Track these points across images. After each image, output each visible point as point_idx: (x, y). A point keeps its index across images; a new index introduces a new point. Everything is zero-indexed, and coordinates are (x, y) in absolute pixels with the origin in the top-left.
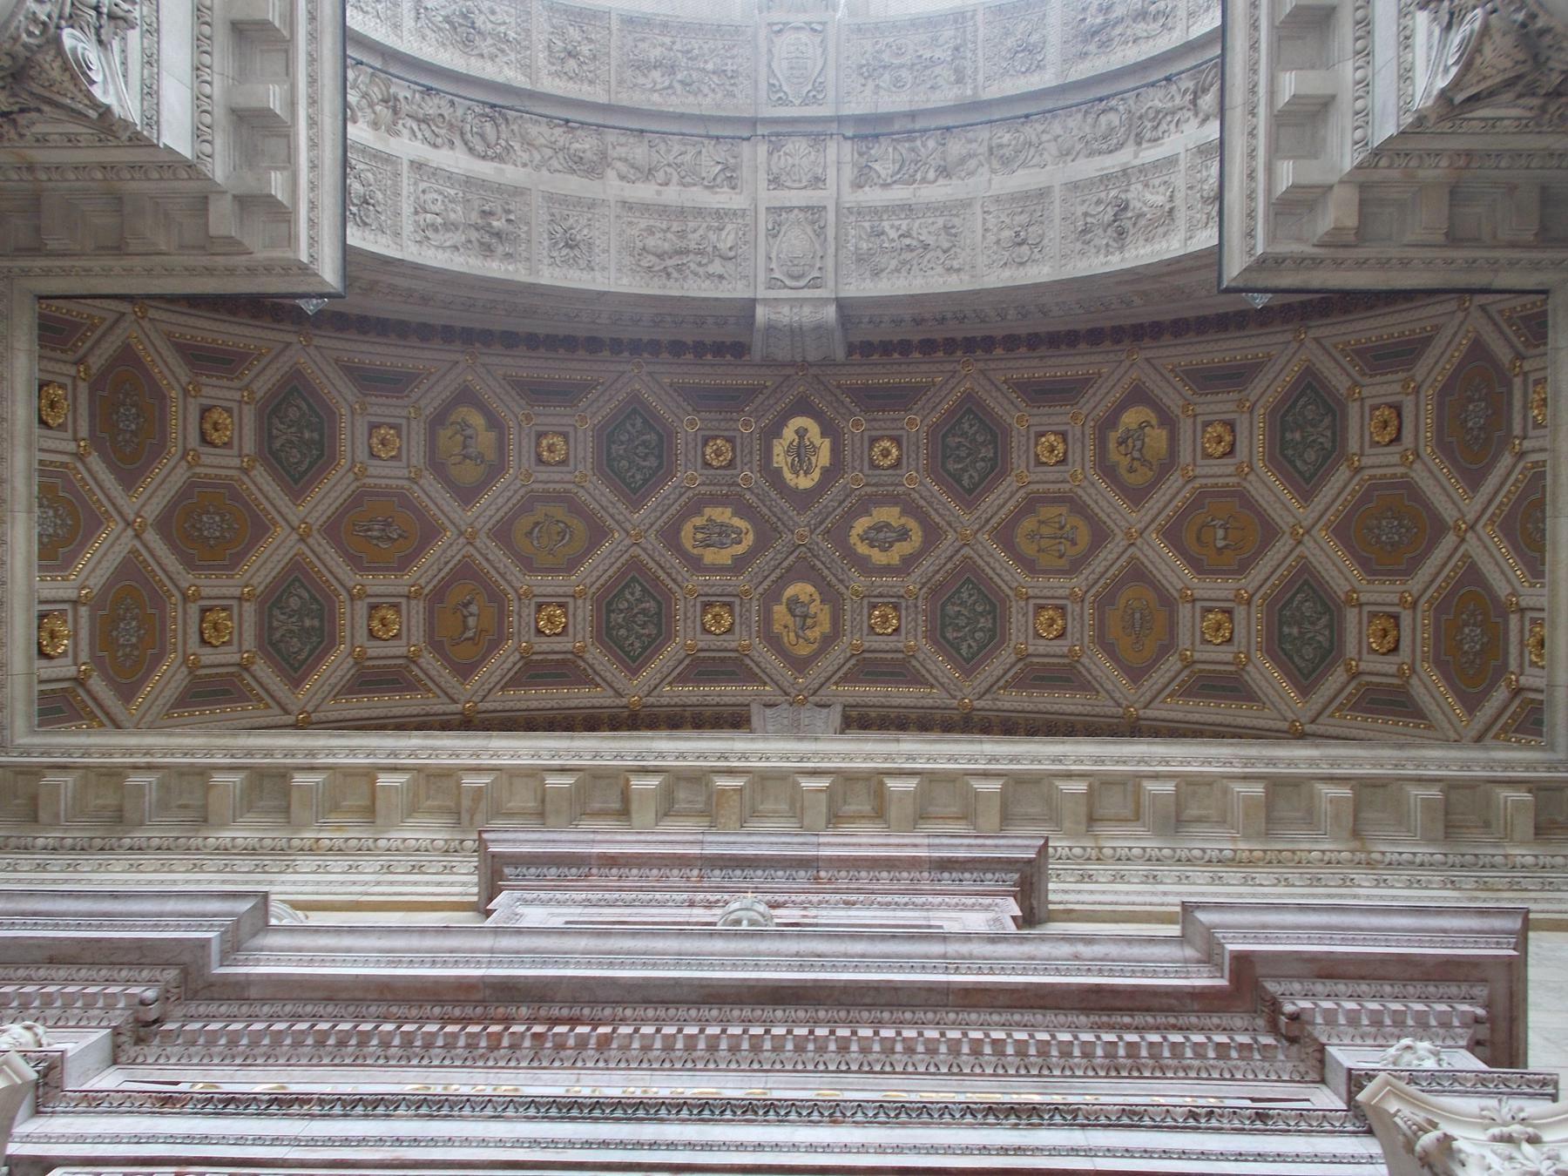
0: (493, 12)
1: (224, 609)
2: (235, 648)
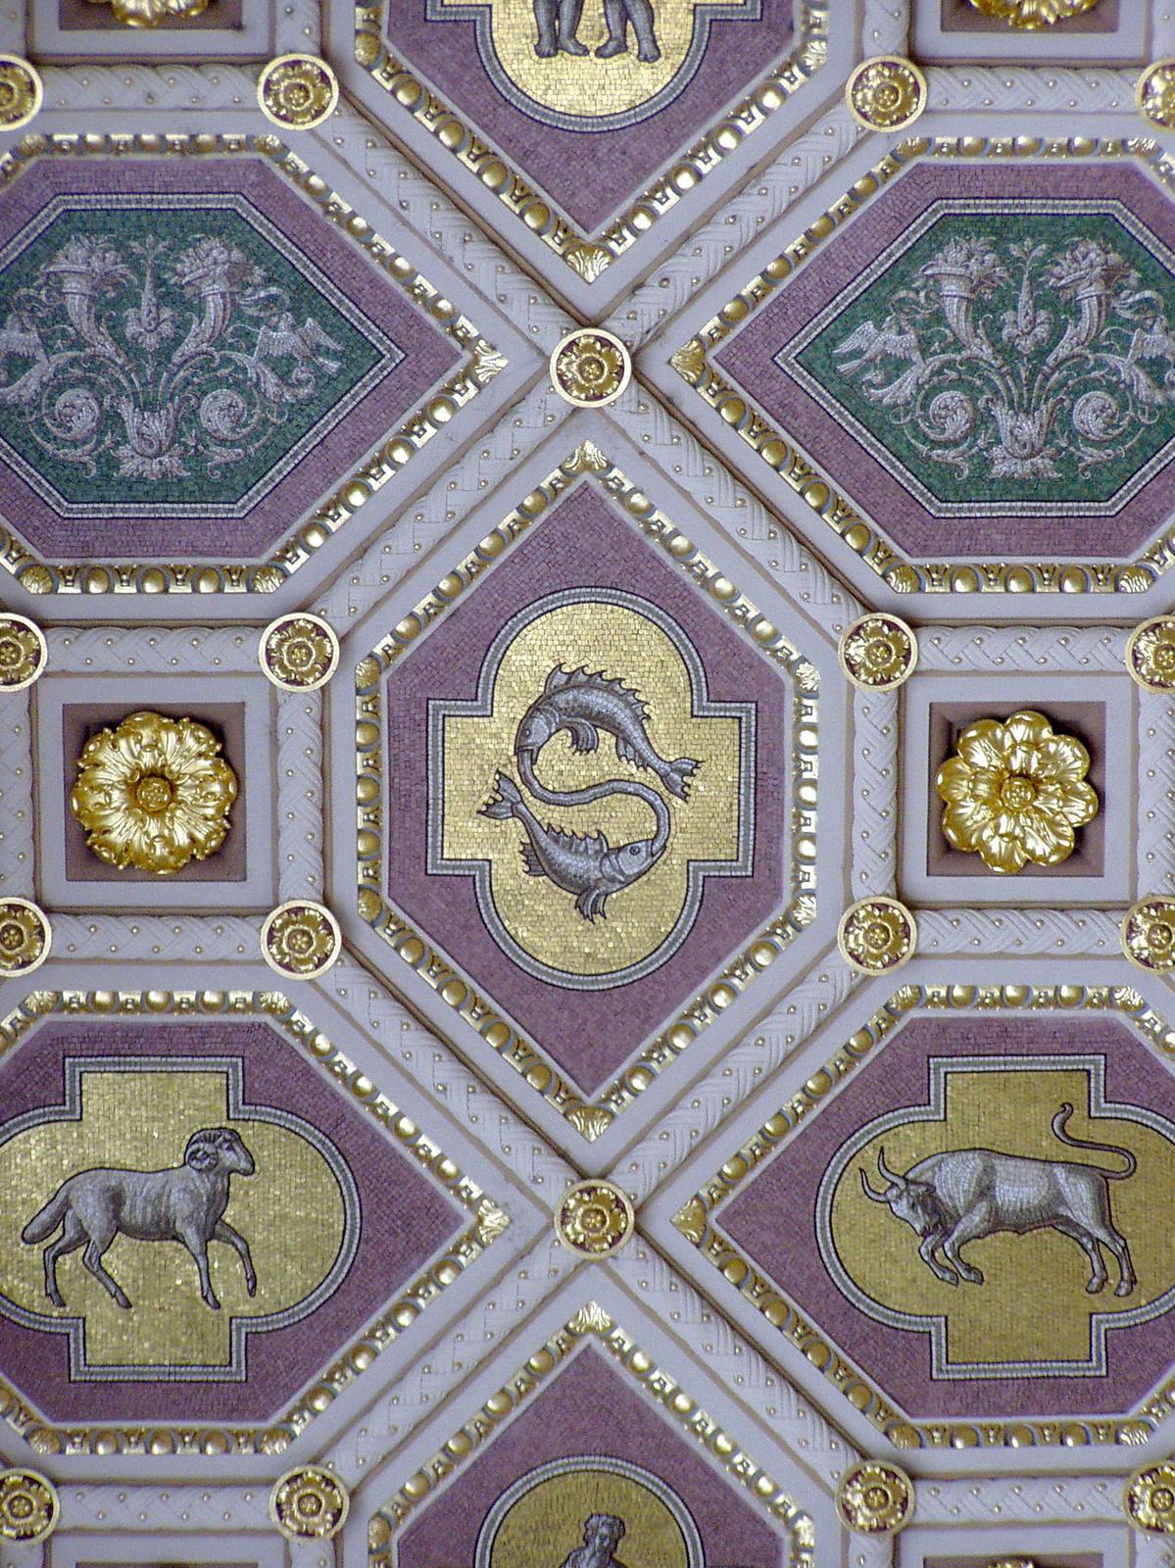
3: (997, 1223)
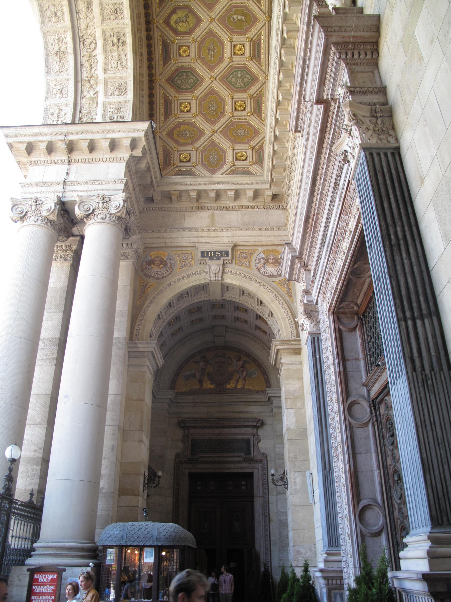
0: (52, 44)
1: (235, 104)
2: (246, 100)
3: (238, 20)
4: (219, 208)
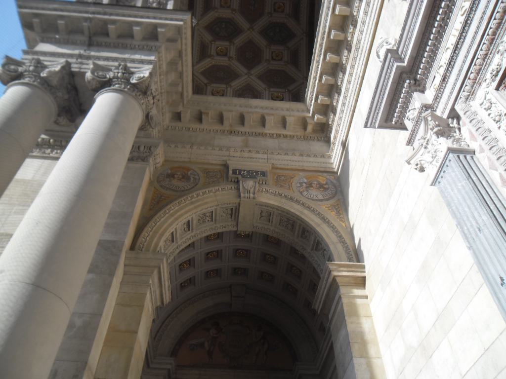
4: (254, 134)
